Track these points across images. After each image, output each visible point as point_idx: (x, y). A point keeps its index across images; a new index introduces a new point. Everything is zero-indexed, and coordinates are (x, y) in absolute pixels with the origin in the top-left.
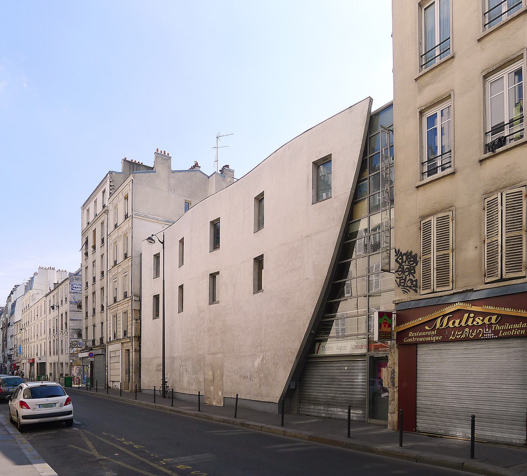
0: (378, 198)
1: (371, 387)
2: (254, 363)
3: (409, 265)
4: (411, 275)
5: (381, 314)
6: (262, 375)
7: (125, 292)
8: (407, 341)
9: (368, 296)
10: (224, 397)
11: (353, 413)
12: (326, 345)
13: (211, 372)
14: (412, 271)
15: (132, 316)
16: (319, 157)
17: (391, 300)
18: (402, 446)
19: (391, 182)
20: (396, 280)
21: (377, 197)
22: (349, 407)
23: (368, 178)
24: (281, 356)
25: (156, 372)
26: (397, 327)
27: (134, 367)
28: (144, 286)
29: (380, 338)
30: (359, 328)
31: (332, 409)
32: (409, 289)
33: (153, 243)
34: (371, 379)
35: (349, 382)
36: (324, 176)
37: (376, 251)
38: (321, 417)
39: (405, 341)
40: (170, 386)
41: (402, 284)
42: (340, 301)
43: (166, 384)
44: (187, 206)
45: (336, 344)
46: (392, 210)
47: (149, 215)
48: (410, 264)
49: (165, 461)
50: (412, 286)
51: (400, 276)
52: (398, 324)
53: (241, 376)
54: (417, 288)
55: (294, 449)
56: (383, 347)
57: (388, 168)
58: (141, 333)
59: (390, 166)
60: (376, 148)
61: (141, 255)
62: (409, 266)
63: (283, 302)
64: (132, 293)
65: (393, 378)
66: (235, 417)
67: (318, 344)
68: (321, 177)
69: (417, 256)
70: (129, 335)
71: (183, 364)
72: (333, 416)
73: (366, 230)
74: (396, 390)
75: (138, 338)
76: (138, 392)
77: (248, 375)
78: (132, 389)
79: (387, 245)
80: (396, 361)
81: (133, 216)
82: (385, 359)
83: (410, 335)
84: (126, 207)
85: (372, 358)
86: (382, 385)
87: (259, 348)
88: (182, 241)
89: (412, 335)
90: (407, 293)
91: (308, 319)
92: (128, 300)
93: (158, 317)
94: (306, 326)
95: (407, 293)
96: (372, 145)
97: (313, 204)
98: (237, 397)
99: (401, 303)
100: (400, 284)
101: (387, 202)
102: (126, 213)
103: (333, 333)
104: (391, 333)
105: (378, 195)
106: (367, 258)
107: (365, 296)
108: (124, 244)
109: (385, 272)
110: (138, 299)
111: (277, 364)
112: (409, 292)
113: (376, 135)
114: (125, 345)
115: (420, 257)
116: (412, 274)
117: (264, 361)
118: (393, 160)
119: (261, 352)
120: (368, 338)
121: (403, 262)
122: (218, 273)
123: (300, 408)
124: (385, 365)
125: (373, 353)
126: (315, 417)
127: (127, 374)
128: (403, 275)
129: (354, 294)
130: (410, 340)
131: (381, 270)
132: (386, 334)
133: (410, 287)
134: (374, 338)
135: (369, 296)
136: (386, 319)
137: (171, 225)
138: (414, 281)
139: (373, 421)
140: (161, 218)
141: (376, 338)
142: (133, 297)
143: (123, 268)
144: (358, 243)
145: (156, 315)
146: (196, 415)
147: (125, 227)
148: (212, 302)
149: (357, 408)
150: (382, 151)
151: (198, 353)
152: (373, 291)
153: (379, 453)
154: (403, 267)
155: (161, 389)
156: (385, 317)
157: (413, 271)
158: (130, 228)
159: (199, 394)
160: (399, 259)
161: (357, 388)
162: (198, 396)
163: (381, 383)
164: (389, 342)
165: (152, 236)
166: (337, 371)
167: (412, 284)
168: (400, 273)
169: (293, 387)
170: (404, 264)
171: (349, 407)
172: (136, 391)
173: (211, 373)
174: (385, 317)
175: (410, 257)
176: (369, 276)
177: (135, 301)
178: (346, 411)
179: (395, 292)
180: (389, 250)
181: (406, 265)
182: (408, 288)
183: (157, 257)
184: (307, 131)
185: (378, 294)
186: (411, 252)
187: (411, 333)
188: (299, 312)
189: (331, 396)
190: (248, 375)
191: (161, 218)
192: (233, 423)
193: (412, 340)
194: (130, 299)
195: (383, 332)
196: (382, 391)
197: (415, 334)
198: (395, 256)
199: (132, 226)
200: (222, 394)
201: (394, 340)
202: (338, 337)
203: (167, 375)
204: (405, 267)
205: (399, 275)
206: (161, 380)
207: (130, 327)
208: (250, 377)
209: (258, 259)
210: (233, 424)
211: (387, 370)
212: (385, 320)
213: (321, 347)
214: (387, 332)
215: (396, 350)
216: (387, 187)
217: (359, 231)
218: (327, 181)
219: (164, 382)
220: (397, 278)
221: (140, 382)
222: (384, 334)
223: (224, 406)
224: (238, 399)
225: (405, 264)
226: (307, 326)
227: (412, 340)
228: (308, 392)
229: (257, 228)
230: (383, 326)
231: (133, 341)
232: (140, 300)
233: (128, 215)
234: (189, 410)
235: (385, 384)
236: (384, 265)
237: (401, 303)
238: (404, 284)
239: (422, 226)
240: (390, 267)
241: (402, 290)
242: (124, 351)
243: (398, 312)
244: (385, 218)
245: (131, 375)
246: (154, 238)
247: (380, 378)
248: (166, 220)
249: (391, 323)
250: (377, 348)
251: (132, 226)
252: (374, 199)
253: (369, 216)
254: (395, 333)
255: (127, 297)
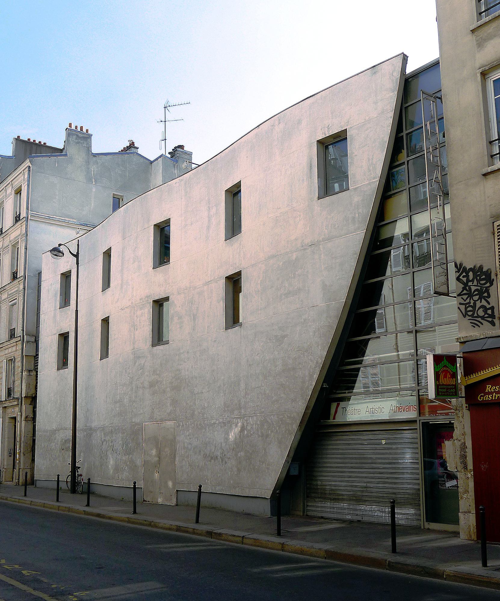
0: (422, 190)
1: (427, 472)
2: (228, 435)
3: (479, 285)
4: (483, 299)
5: (438, 359)
6: (242, 454)
7: (11, 330)
8: (483, 398)
9: (414, 332)
10: (177, 491)
11: (398, 514)
12: (349, 406)
13: (155, 450)
14: (484, 294)
15: (22, 365)
16: (327, 133)
17: (455, 336)
18: (487, 567)
19: (443, 168)
20: (459, 308)
21: (422, 188)
22: (391, 502)
23: (406, 163)
24: (273, 424)
25: (60, 452)
26: (465, 377)
27: (22, 445)
28: (44, 320)
29: (437, 395)
30: (401, 379)
31: (363, 507)
32: (482, 321)
33: (60, 256)
34: (427, 459)
35: (390, 463)
36: (335, 159)
37: (424, 265)
38: (343, 521)
39: (480, 399)
40: (84, 475)
41: (470, 313)
42: (369, 339)
43: (78, 472)
44: (117, 203)
45: (365, 405)
46: (447, 208)
47: (54, 217)
48: (480, 284)
49: (75, 597)
50: (486, 316)
51: (465, 301)
52: (467, 372)
53: (205, 456)
54: (495, 319)
55: (300, 573)
56: (444, 408)
57: (437, 148)
58: (37, 391)
59: (439, 146)
60: (415, 121)
61: (40, 274)
62: (479, 286)
63: (274, 341)
64: (23, 330)
65: (464, 457)
66: (197, 522)
67: (334, 406)
68: (330, 161)
69: (491, 272)
70: (17, 395)
71: (108, 438)
72: (366, 519)
73: (405, 235)
74: (469, 475)
75: (33, 399)
76: (29, 485)
77: (219, 454)
78: (19, 479)
79: (441, 256)
80: (468, 430)
81: (29, 219)
82: (449, 427)
83: (488, 390)
84: (17, 204)
85: (426, 426)
86: (446, 469)
87: (236, 412)
88: (108, 254)
89: (491, 389)
90: (479, 327)
91: (316, 367)
92: (16, 342)
93: (66, 367)
94: (313, 376)
95: (479, 327)
96: (410, 117)
97: (319, 198)
98: (200, 489)
99: (470, 341)
100: (466, 314)
101: (438, 196)
102: (18, 214)
103: (358, 387)
104: (455, 387)
105: (423, 187)
106: (410, 276)
107: (409, 332)
108: (13, 258)
109: (440, 295)
110: (33, 339)
111: (267, 436)
112: (482, 324)
113: (415, 104)
114: (9, 410)
115: (497, 274)
116: (484, 298)
117: (246, 431)
118: (444, 137)
119: (240, 418)
120: (419, 395)
121: (468, 281)
122: (167, 299)
123: (307, 505)
124: (450, 437)
125: (427, 417)
126: (335, 520)
127: (10, 456)
128: (470, 300)
129: (391, 327)
130: (488, 397)
131: (434, 293)
132: (447, 389)
133: (483, 318)
134: (428, 395)
135: (416, 332)
136: (447, 365)
137: (90, 231)
138: (489, 309)
139: (434, 526)
140: (74, 220)
141: (431, 393)
142: (25, 337)
143: (10, 293)
144: (395, 254)
145: (63, 363)
146: (129, 521)
147: (16, 233)
148: (157, 342)
149: (405, 504)
150: (426, 125)
151: (133, 420)
152: (423, 323)
153: (449, 577)
154: (470, 289)
155: (69, 479)
156: (445, 362)
157: (486, 294)
158: (23, 235)
159: (135, 486)
160: (462, 275)
161: (403, 473)
162: (133, 490)
163: (444, 465)
164: (454, 401)
165: (59, 246)
166: (369, 446)
167: (486, 313)
168: (465, 297)
169: (295, 472)
170: (470, 284)
171: (391, 502)
172: (26, 484)
173: (154, 452)
174: (445, 362)
175: (479, 273)
176: (415, 301)
177: (28, 342)
178: (387, 510)
179: (459, 325)
180: (444, 264)
181: (474, 286)
182: (479, 319)
183: (66, 276)
184: (307, 98)
185: (430, 329)
186: (481, 267)
187: (489, 387)
188: (302, 356)
189: (362, 487)
190: (219, 454)
191: (74, 220)
192: (194, 532)
193: (492, 398)
194: (20, 340)
195: (443, 385)
196: (447, 478)
197: (495, 388)
198: (456, 272)
199: (26, 232)
200: (174, 484)
201: (462, 397)
202: (367, 393)
203: (80, 455)
204: (473, 288)
205: (464, 299)
206: (69, 464)
207: (18, 383)
208: (221, 457)
209: (233, 278)
210: (194, 533)
211: (454, 444)
212: (445, 366)
213: (340, 409)
214: (450, 385)
215: (467, 414)
216: (437, 174)
217: (395, 237)
218: (341, 167)
219: (74, 468)
220: (461, 304)
221: (32, 469)
222: (445, 388)
223: (177, 505)
224: (202, 493)
225: (473, 284)
226: (316, 376)
227: (489, 396)
228: (321, 481)
229: (231, 234)
230: (441, 376)
231: (23, 404)
232: (37, 342)
233: (20, 216)
234: (116, 512)
235: (451, 467)
236: (439, 285)
237: (470, 341)
238: (473, 314)
239: (496, 230)
240: (448, 288)
241: (470, 323)
242: (7, 420)
243: (465, 355)
244: (436, 218)
245: (17, 457)
246: (62, 248)
247: (441, 457)
248: (82, 223)
249: (454, 371)
250: (433, 410)
251: (26, 232)
252: (417, 192)
253: (411, 216)
254: (463, 388)
255: (14, 337)
